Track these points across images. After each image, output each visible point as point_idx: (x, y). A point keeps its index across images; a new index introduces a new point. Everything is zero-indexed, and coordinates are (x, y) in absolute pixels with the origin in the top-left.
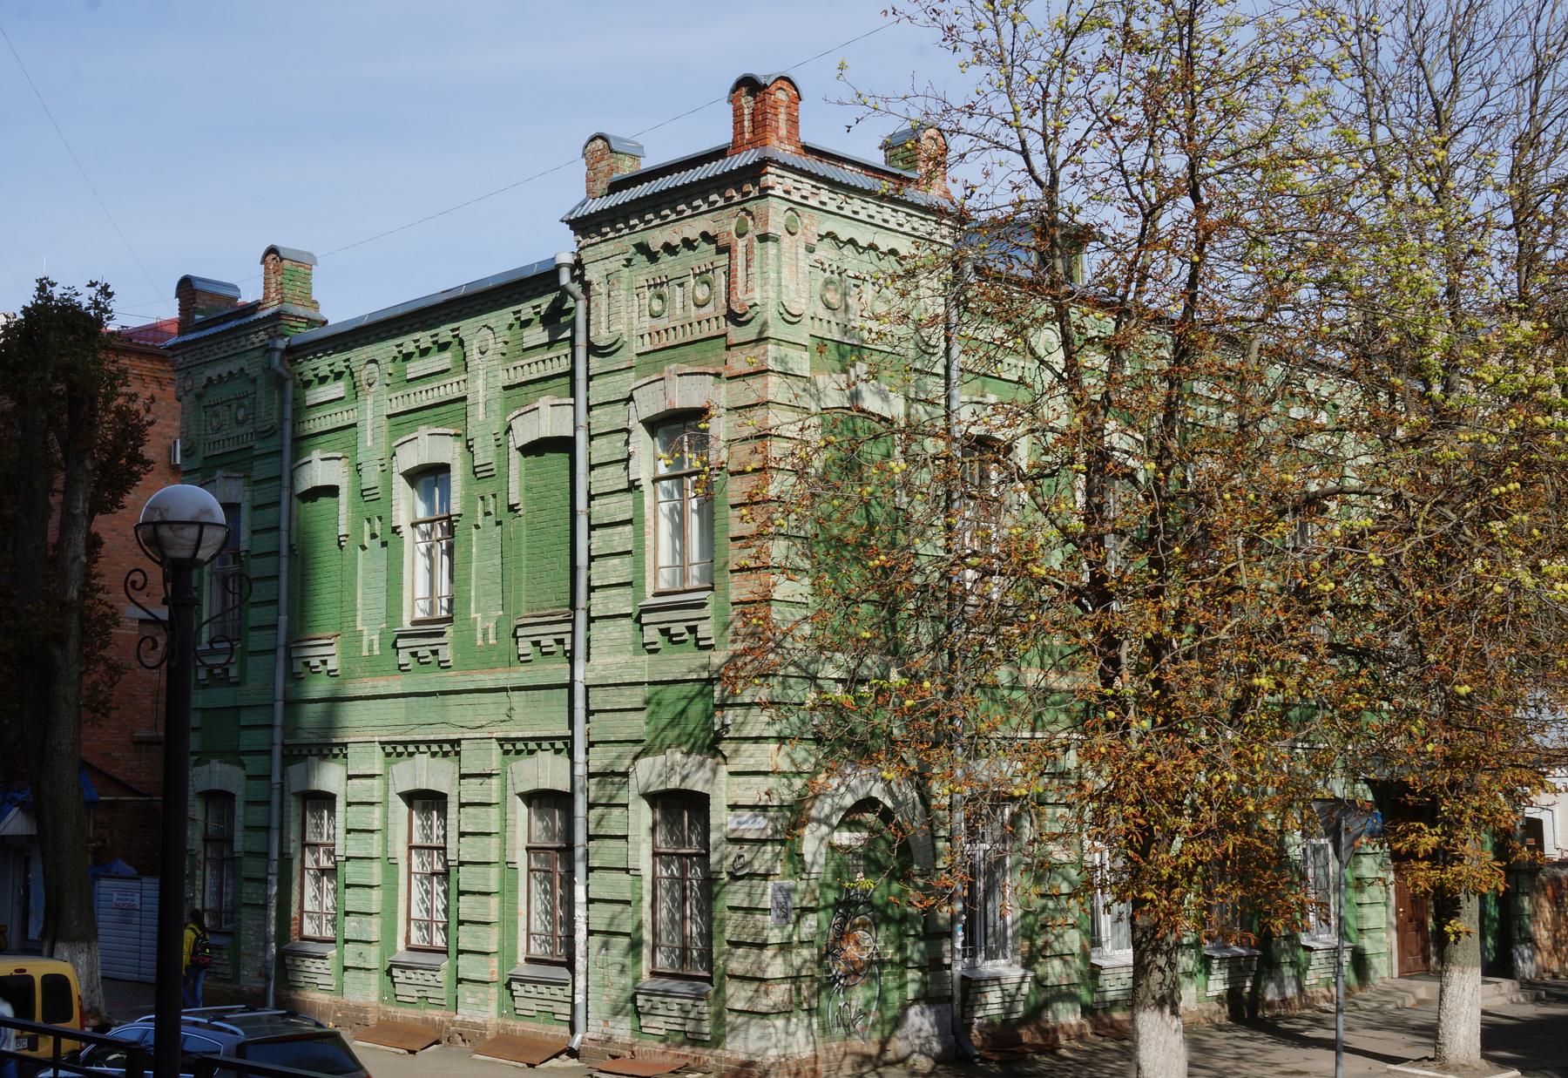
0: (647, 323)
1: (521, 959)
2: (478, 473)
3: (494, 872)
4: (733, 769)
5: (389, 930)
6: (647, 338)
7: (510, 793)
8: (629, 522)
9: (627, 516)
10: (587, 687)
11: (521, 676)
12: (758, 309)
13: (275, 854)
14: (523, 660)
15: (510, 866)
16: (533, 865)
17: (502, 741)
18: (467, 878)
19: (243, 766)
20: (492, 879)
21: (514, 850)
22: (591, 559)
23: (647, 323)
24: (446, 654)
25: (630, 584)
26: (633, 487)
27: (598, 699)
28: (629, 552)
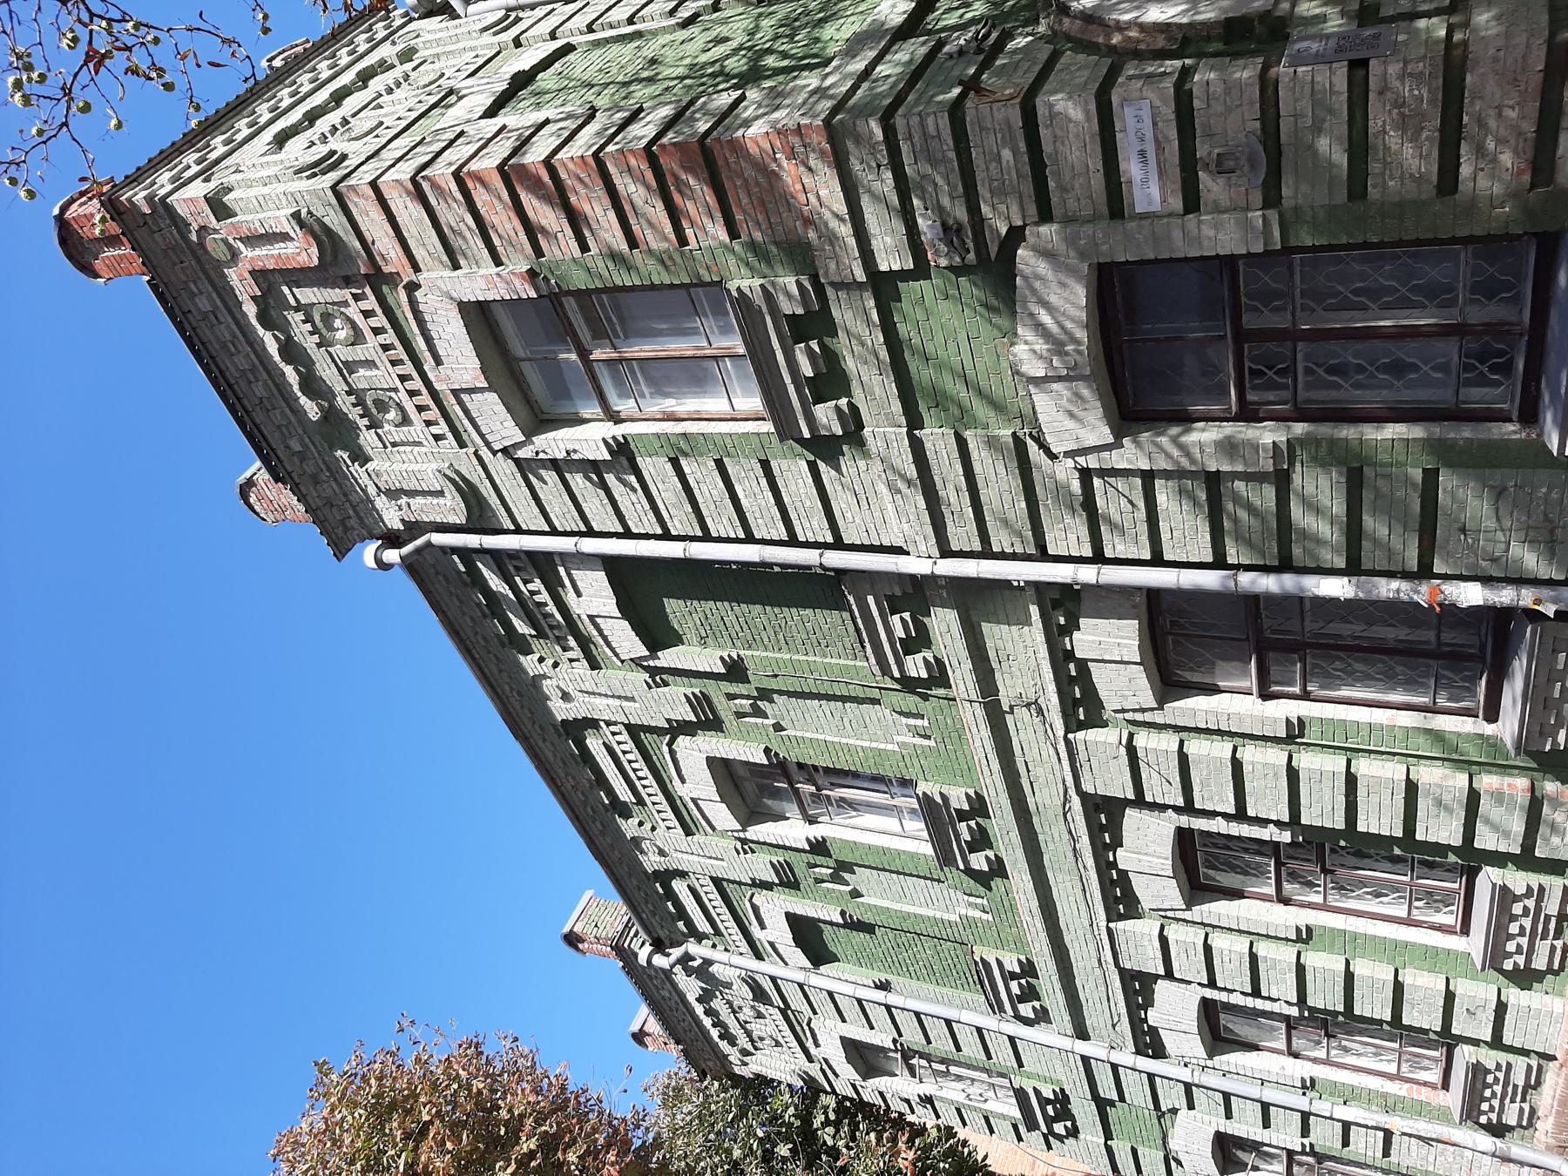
0: (417, 430)
1: (1490, 729)
2: (713, 724)
3: (1307, 761)
4: (1032, 210)
5: (1430, 958)
6: (435, 430)
7: (1158, 717)
8: (675, 463)
9: (669, 466)
10: (946, 552)
11: (962, 677)
12: (304, 212)
13: (1302, 1103)
14: (939, 675)
15: (1294, 734)
16: (1297, 690)
17: (1072, 724)
18: (1324, 811)
19: (1174, 1111)
20: (1317, 764)
21: (1263, 721)
22: (750, 539)
23: (417, 430)
24: (959, 800)
25: (765, 464)
26: (623, 454)
27: (962, 534)
28: (720, 464)
